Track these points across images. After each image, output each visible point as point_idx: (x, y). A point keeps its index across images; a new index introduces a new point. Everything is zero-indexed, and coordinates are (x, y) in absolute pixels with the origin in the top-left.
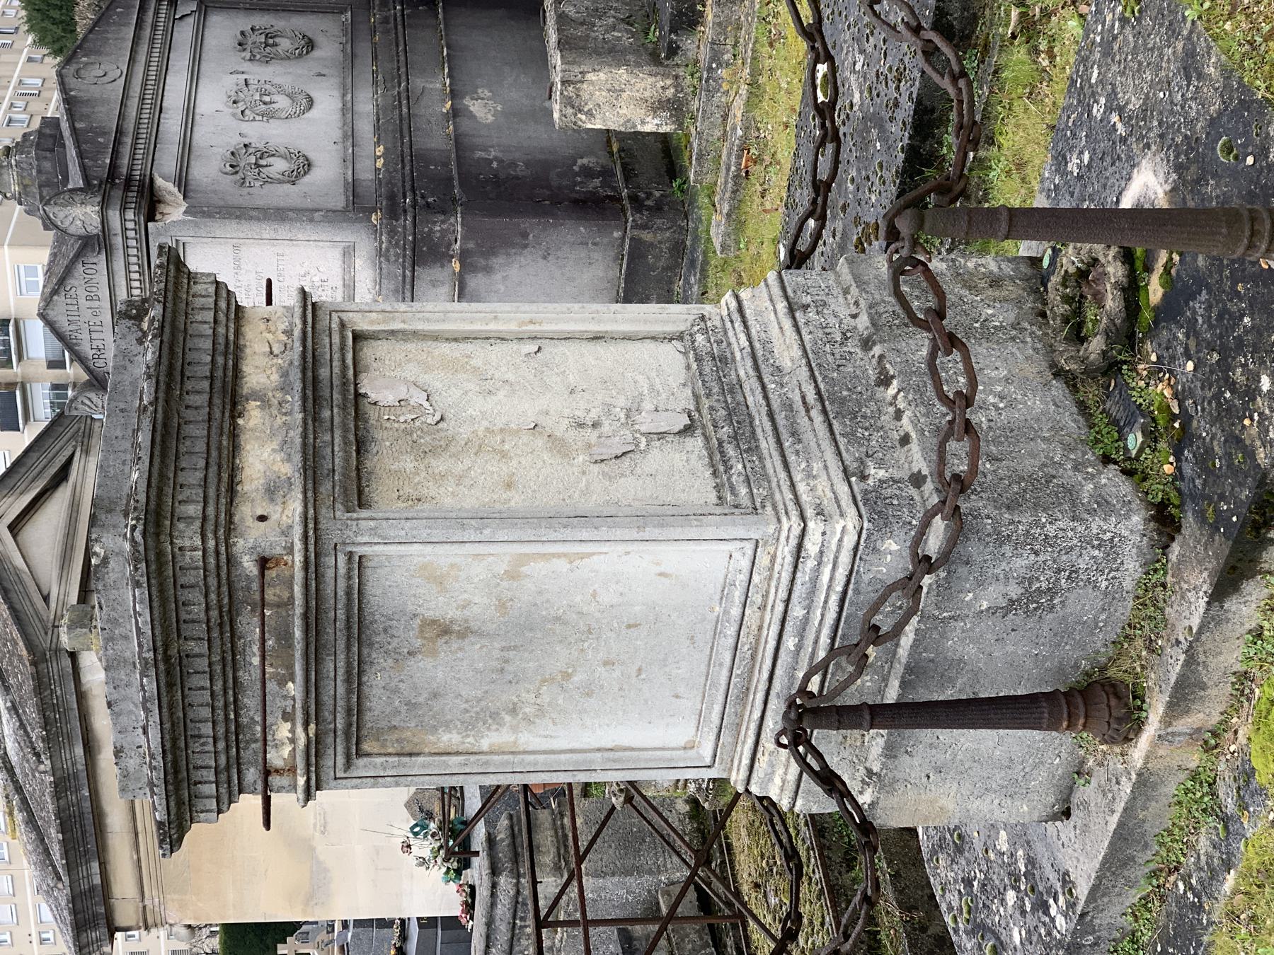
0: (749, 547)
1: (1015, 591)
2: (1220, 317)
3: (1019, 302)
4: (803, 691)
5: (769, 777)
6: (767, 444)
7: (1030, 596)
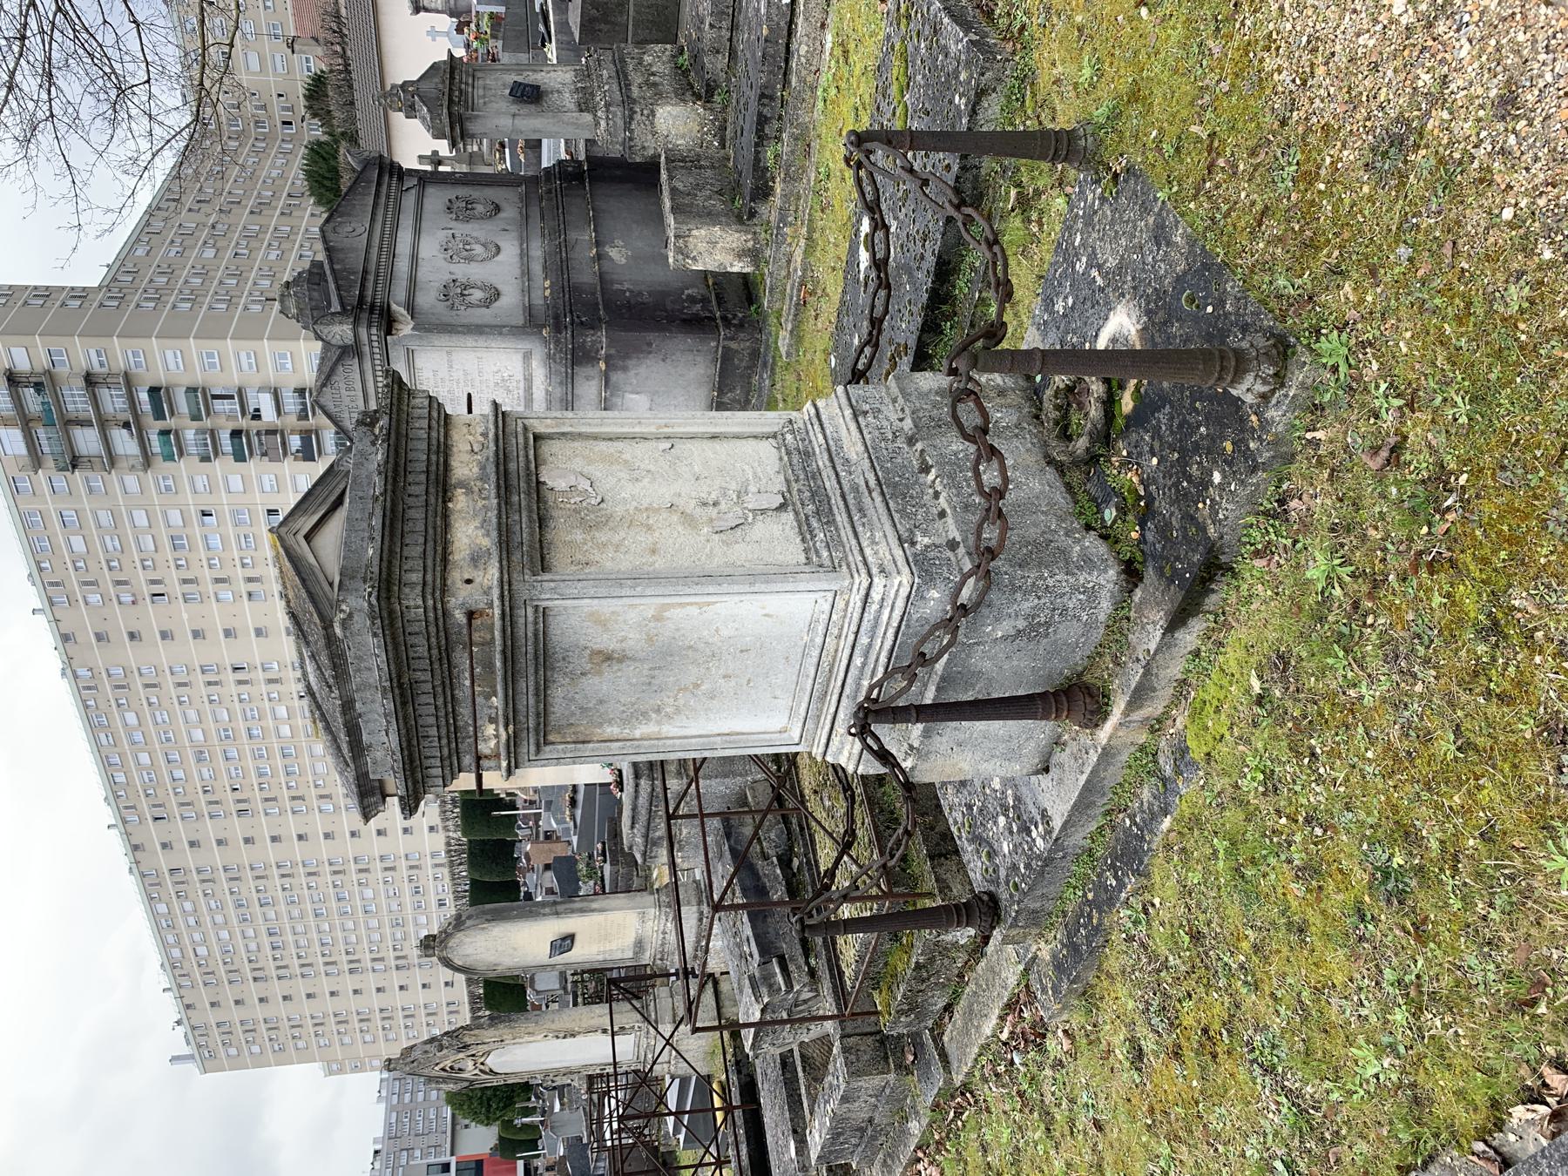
0: (830, 596)
1: (1021, 624)
2: (1180, 426)
3: (1020, 408)
4: (868, 698)
5: (840, 751)
6: (841, 518)
7: (1032, 627)
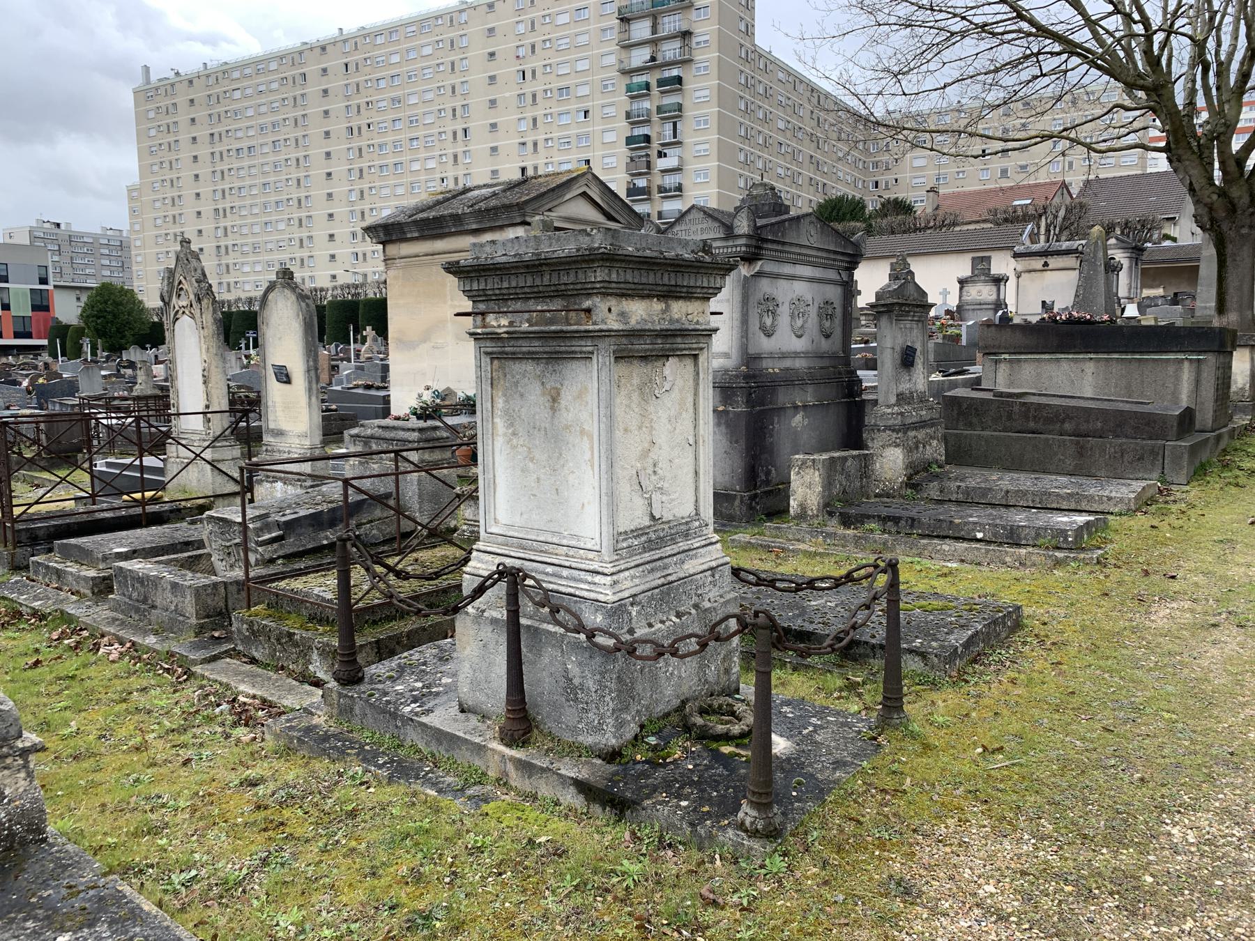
0: (597, 548)
1: (576, 681)
2: (715, 781)
3: (717, 683)
4: (526, 576)
5: (481, 561)
6: (647, 556)
7: (574, 690)
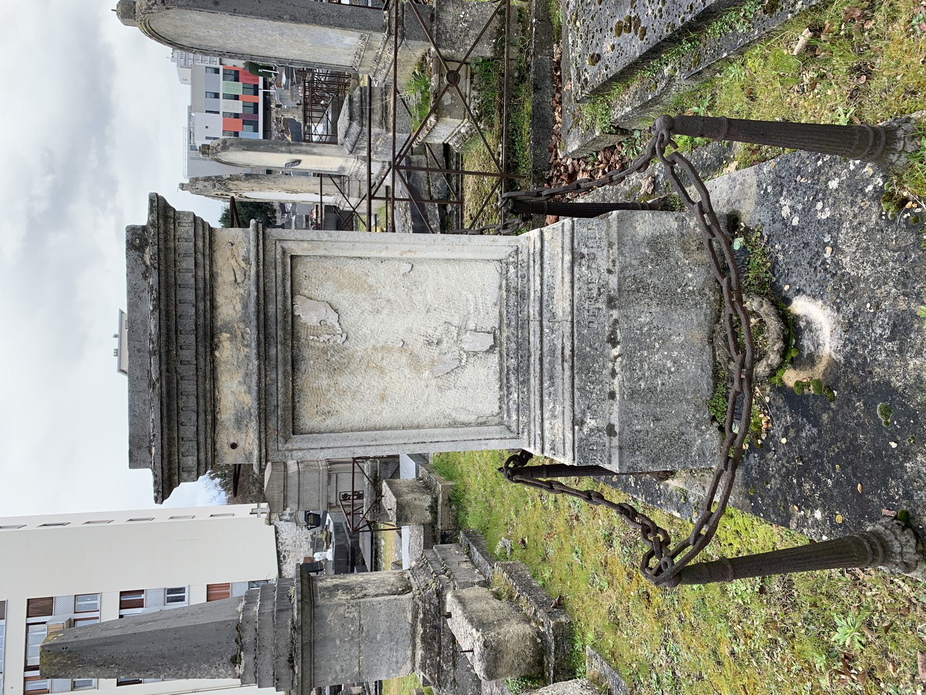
6: (534, 382)
